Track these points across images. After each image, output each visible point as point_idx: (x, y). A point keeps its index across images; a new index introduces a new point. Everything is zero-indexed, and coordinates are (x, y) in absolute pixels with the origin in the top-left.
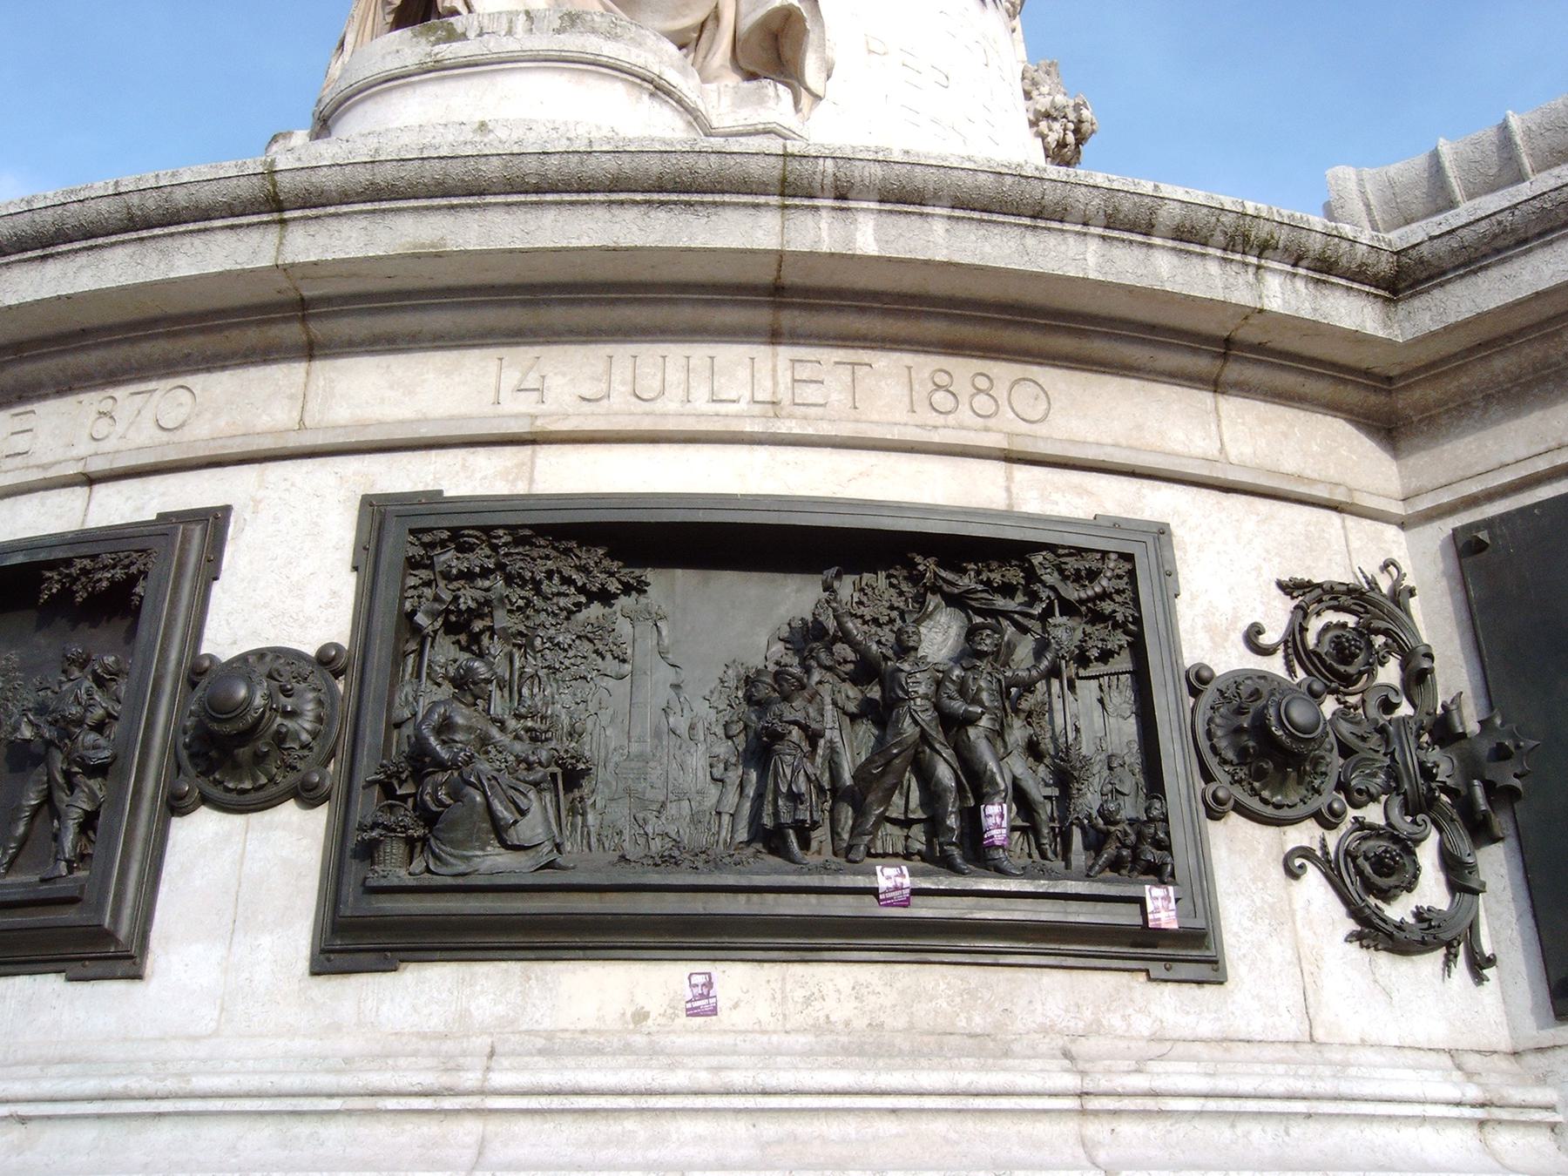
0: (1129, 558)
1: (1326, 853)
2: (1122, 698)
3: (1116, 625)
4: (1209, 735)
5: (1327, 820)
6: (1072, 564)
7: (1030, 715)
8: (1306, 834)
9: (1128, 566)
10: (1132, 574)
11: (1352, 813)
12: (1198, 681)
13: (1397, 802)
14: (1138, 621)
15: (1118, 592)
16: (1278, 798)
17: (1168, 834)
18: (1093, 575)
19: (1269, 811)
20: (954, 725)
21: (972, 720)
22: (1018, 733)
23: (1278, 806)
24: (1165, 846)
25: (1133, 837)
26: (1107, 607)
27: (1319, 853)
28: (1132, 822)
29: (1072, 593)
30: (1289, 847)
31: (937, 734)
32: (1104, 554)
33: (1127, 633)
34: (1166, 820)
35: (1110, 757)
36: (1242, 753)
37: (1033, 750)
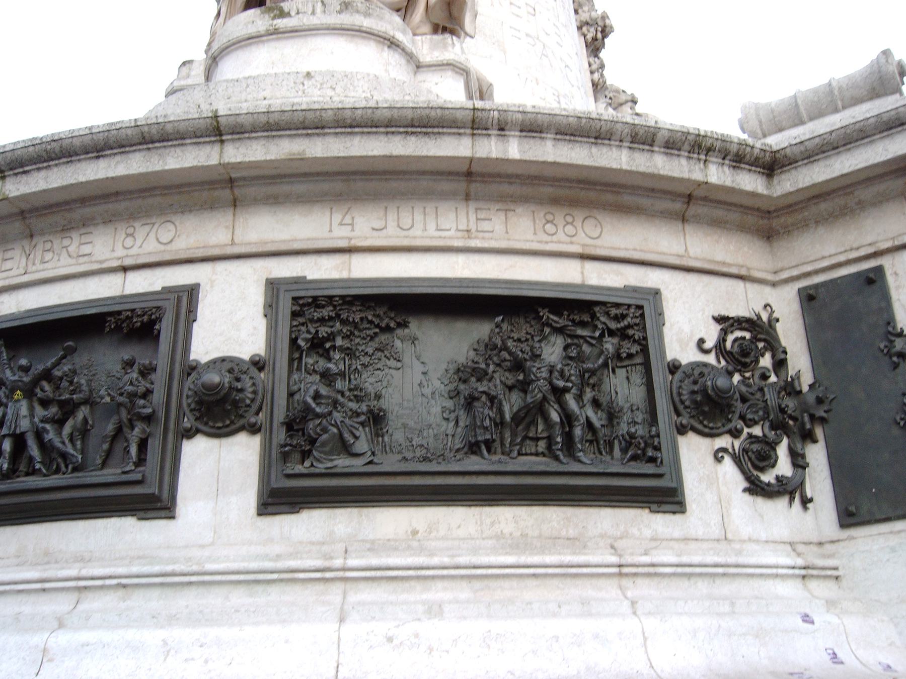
0: (640, 307)
1: (734, 450)
2: (637, 378)
3: (635, 341)
4: (680, 394)
5: (735, 433)
6: (614, 311)
7: (594, 386)
8: (724, 441)
9: (640, 312)
10: (642, 315)
11: (746, 430)
12: (674, 368)
13: (767, 424)
14: (645, 339)
15: (636, 324)
16: (711, 425)
17: (659, 443)
18: (624, 316)
19: (707, 430)
20: (559, 393)
21: (566, 390)
22: (589, 394)
23: (712, 428)
24: (657, 448)
25: (643, 445)
26: (631, 332)
27: (730, 450)
28: (642, 438)
29: (613, 325)
30: (716, 447)
31: (551, 398)
32: (629, 306)
33: (640, 344)
34: (658, 436)
35: (632, 405)
36: (695, 402)
37: (596, 403)
